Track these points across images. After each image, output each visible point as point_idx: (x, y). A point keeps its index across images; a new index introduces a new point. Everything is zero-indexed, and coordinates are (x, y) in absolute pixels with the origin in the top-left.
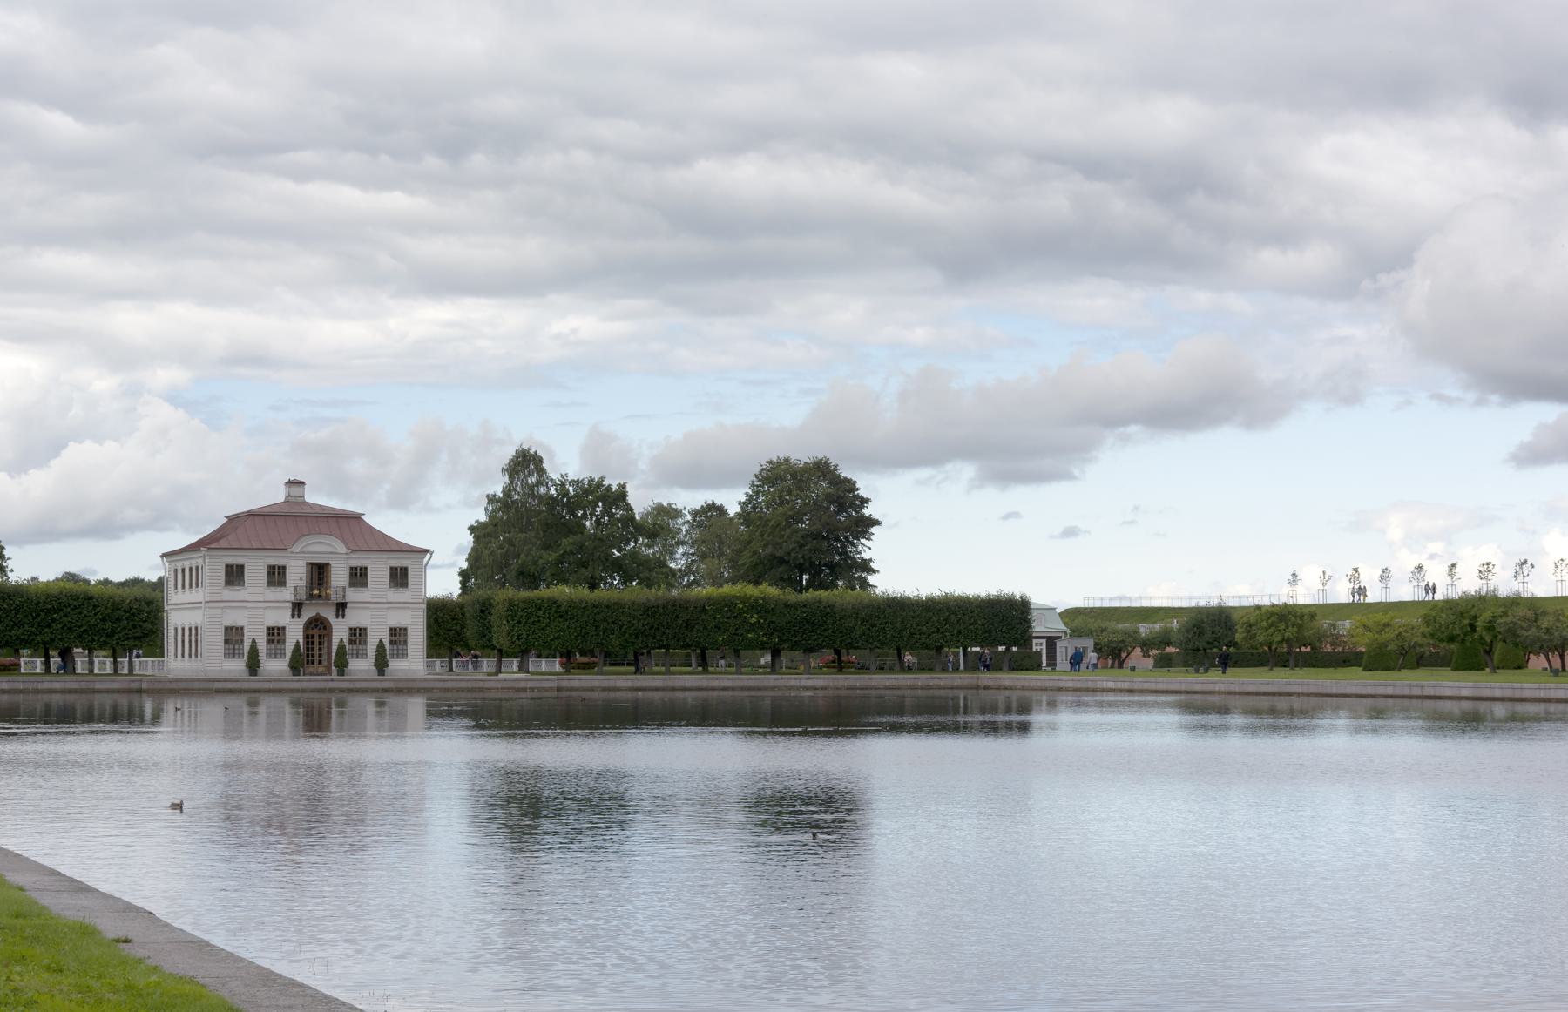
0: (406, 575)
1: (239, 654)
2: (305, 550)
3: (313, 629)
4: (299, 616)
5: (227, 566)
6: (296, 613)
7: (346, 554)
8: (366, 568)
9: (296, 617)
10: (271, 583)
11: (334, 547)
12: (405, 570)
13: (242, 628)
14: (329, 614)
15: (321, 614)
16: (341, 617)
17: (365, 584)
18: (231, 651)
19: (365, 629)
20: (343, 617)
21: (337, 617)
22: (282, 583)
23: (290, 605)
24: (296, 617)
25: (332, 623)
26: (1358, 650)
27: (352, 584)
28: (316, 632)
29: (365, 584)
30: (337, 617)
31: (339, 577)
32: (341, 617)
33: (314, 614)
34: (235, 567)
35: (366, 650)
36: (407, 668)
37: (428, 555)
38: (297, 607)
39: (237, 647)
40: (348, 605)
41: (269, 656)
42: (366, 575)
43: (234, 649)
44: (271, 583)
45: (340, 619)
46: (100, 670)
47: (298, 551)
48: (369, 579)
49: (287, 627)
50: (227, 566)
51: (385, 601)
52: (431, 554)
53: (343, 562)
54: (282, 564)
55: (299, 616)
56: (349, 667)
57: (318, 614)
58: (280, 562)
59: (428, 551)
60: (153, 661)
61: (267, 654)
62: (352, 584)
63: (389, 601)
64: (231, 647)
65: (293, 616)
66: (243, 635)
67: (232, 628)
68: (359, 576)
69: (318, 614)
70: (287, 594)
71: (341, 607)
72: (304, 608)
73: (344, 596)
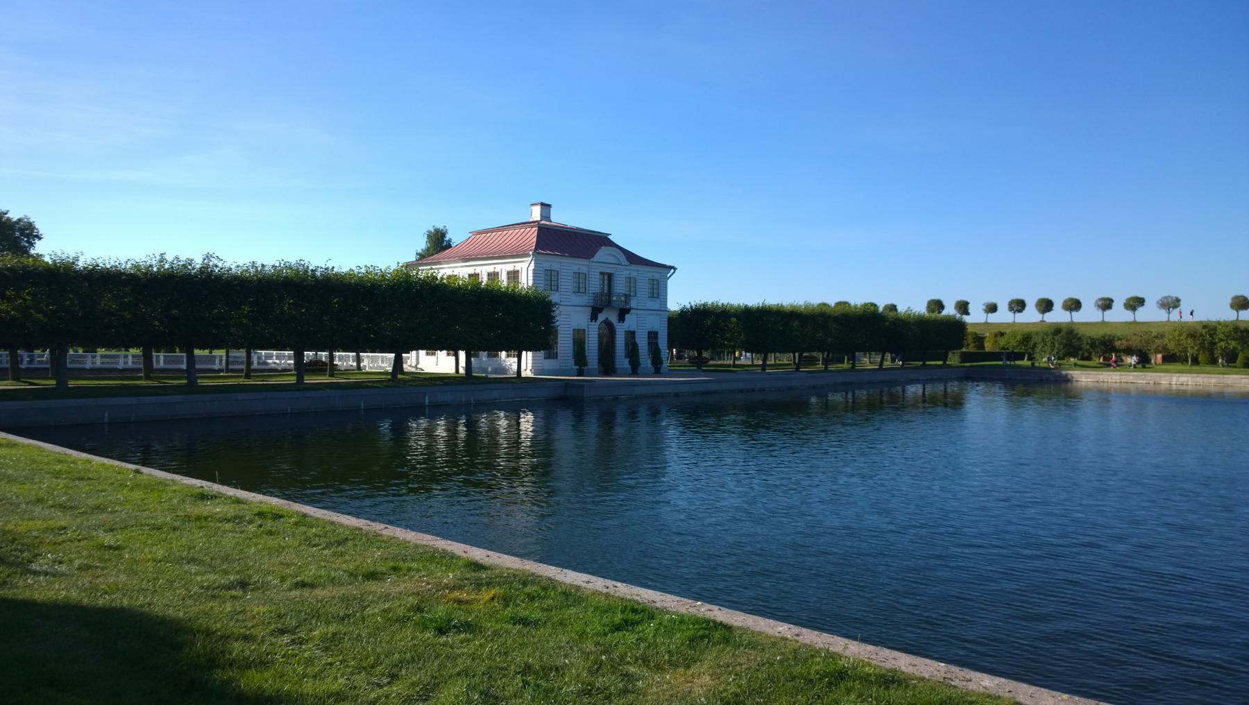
14: (613, 318)
15: (610, 319)
21: (619, 322)
26: (1064, 372)
30: (619, 322)
36: (570, 367)
37: (672, 271)
49: (636, 331)
51: (646, 308)
52: (675, 269)
55: (596, 319)
56: (642, 366)
57: (607, 318)
58: (584, 269)
59: (671, 268)
60: (382, 356)
69: (607, 318)
70: (585, 299)
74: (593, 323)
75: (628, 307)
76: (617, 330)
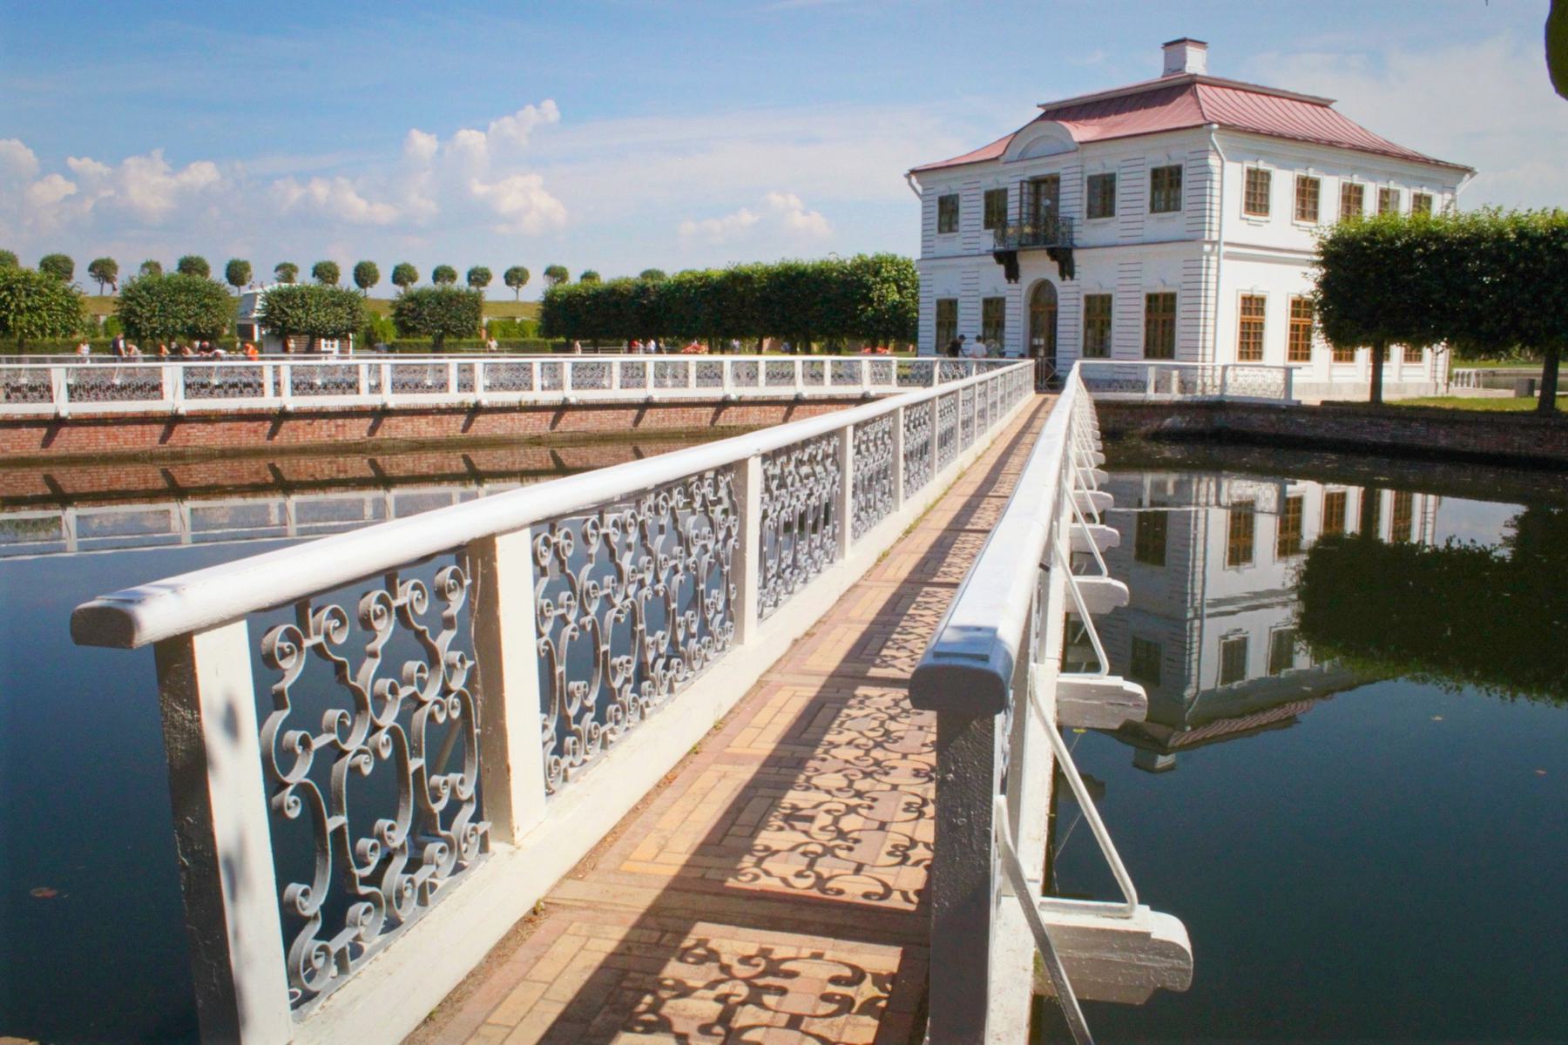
2: (1030, 155)
20: (1072, 278)
21: (1064, 279)
23: (992, 259)
25: (1059, 290)
27: (1091, 214)
30: (1064, 279)
31: (1073, 200)
32: (1067, 277)
38: (1009, 261)
40: (1077, 255)
45: (1068, 281)
46: (471, 368)
62: (1091, 214)
68: (1103, 195)
71: (1065, 260)
74: (1013, 285)
76: (1060, 296)
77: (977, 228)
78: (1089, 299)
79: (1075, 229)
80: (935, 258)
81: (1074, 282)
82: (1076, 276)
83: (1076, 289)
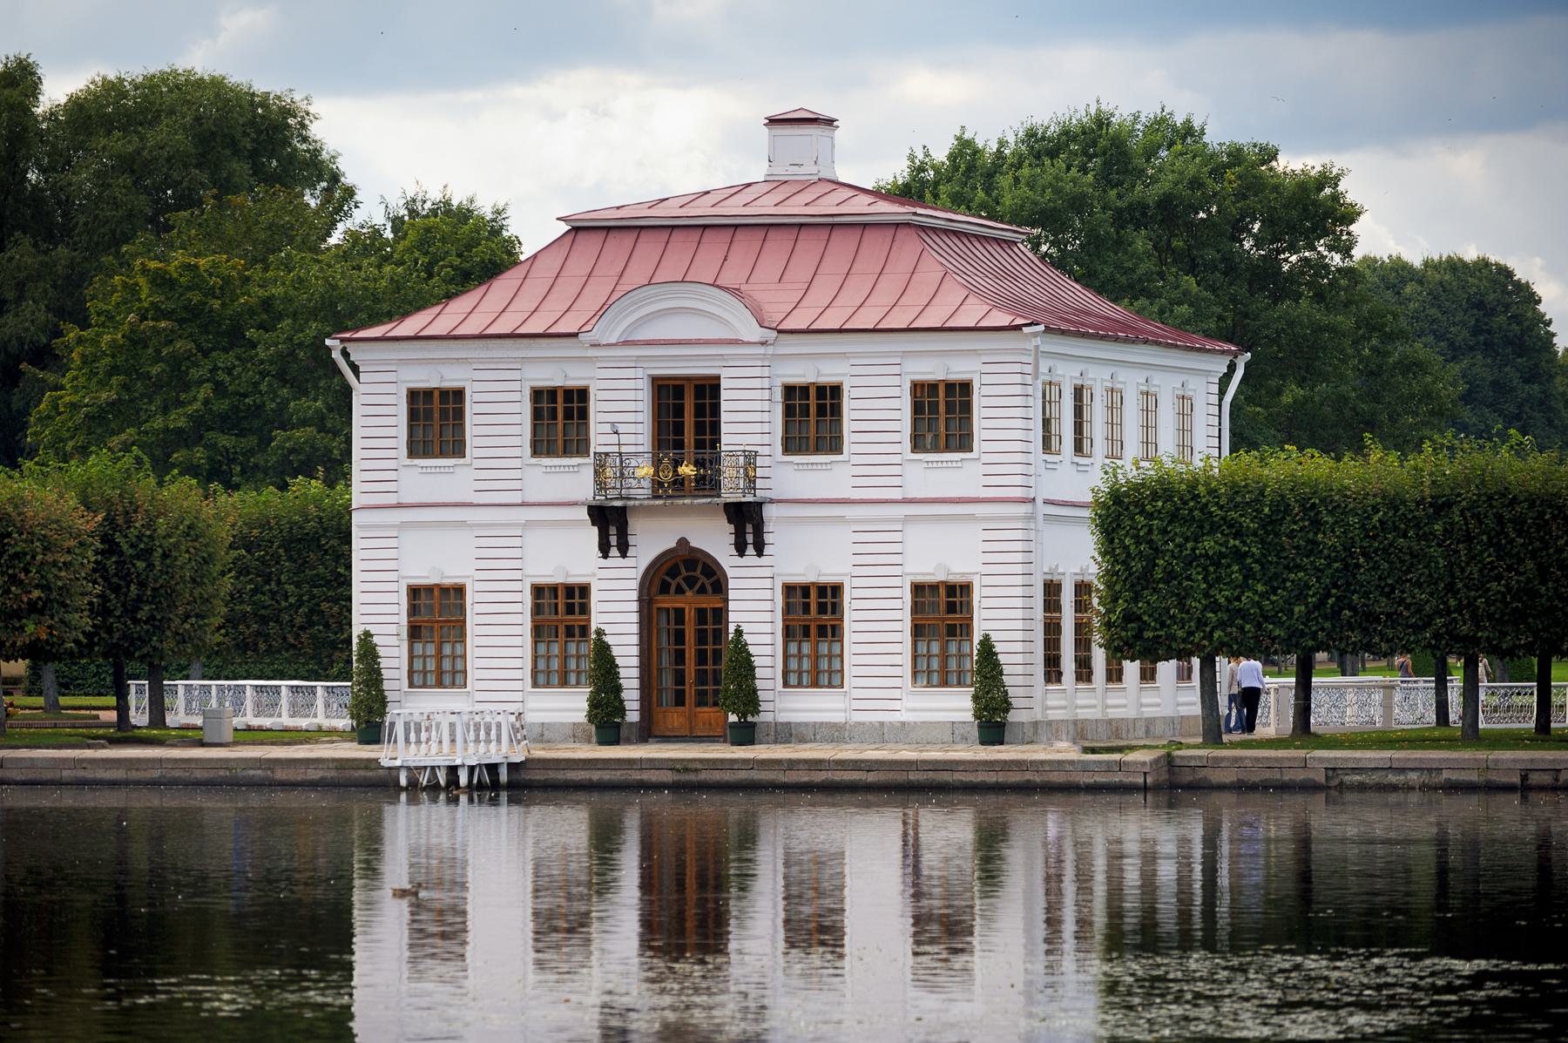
0: (967, 407)
1: (830, 672)
3: (680, 590)
4: (624, 555)
5: (413, 395)
6: (613, 540)
7: (763, 344)
8: (836, 390)
9: (614, 552)
10: (541, 446)
11: (726, 323)
12: (960, 392)
13: (460, 590)
16: (750, 550)
17: (830, 443)
18: (431, 665)
19: (837, 589)
20: (760, 553)
21: (741, 549)
22: (576, 445)
23: (583, 514)
24: (614, 552)
25: (730, 573)
27: (792, 445)
28: (689, 602)
29: (830, 443)
32: (750, 550)
33: (673, 544)
34: (436, 394)
35: (841, 656)
39: (447, 650)
40: (769, 512)
41: (417, 678)
42: (837, 411)
43: (565, 658)
44: (541, 446)
45: (750, 558)
47: (613, 340)
48: (847, 426)
50: (413, 395)
51: (896, 494)
53: (757, 372)
54: (573, 382)
55: (624, 550)
57: (683, 542)
61: (535, 673)
62: (792, 445)
63: (910, 495)
64: (431, 649)
65: (604, 550)
66: (462, 609)
67: (429, 589)
69: (683, 542)
72: (631, 521)
73: (751, 482)
74: (615, 559)
75: (749, 498)
77: (517, 452)
78: (789, 589)
79: (759, 472)
80: (399, 506)
81: (763, 561)
82: (767, 550)
83: (767, 572)
